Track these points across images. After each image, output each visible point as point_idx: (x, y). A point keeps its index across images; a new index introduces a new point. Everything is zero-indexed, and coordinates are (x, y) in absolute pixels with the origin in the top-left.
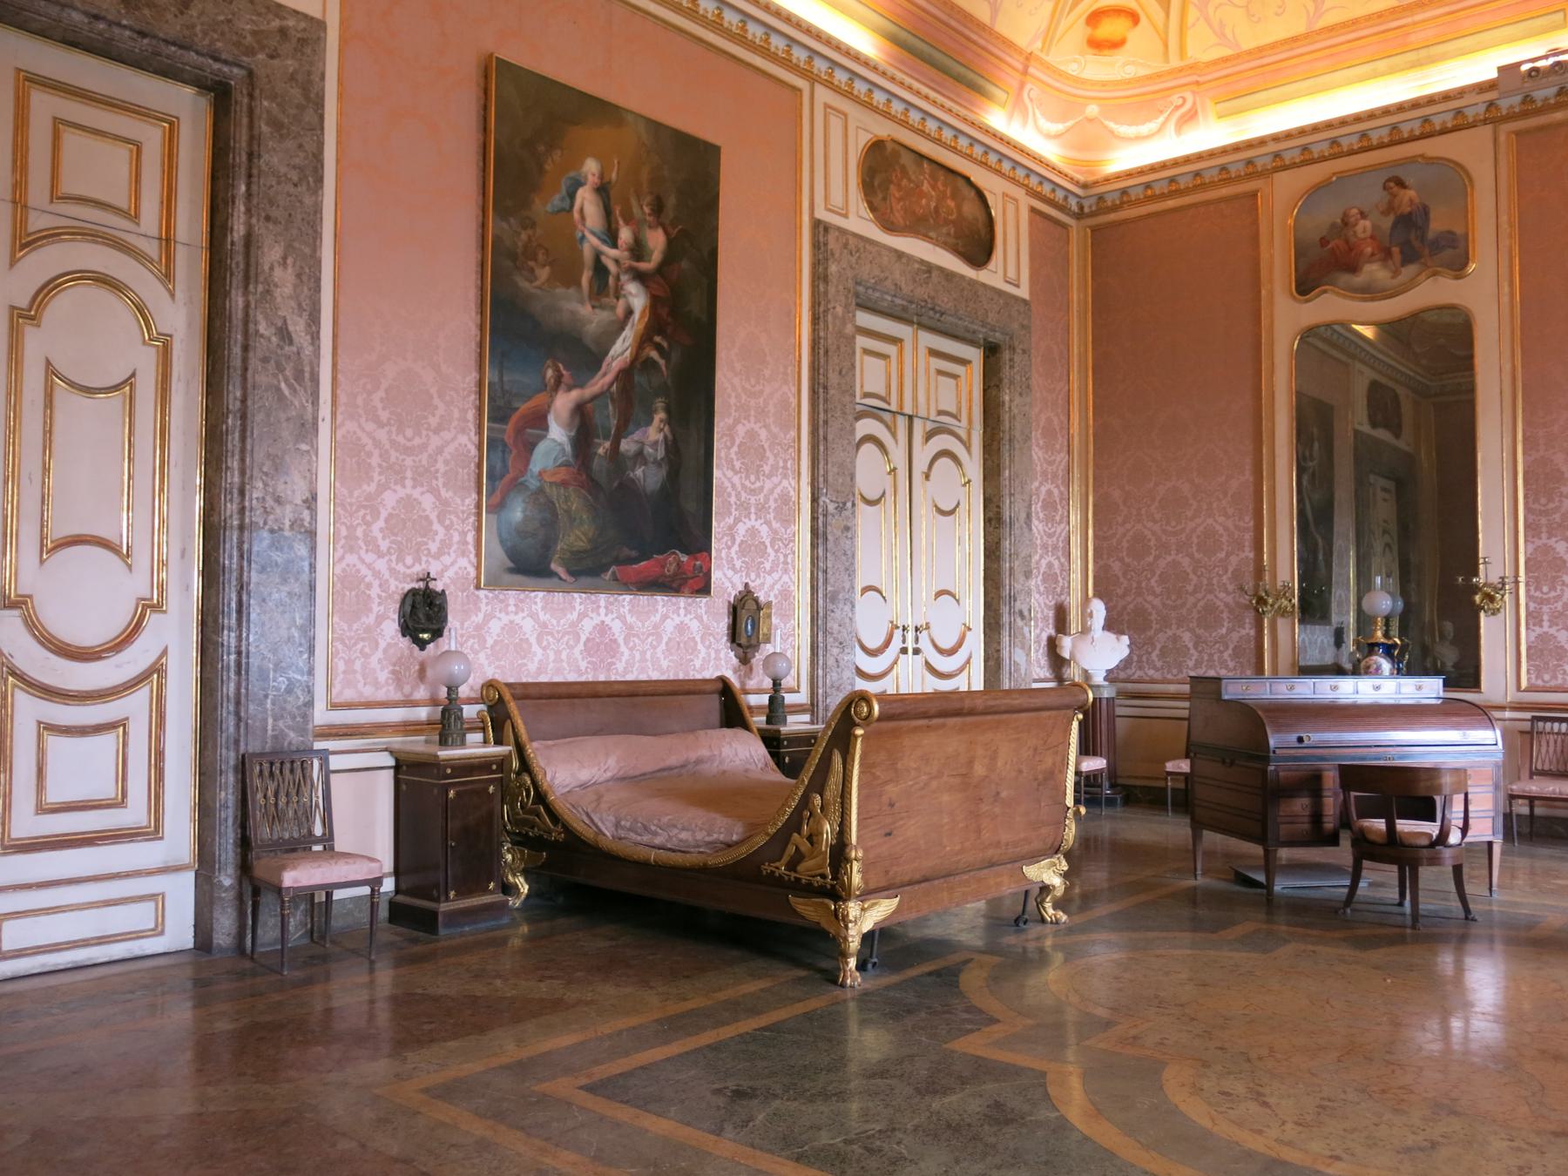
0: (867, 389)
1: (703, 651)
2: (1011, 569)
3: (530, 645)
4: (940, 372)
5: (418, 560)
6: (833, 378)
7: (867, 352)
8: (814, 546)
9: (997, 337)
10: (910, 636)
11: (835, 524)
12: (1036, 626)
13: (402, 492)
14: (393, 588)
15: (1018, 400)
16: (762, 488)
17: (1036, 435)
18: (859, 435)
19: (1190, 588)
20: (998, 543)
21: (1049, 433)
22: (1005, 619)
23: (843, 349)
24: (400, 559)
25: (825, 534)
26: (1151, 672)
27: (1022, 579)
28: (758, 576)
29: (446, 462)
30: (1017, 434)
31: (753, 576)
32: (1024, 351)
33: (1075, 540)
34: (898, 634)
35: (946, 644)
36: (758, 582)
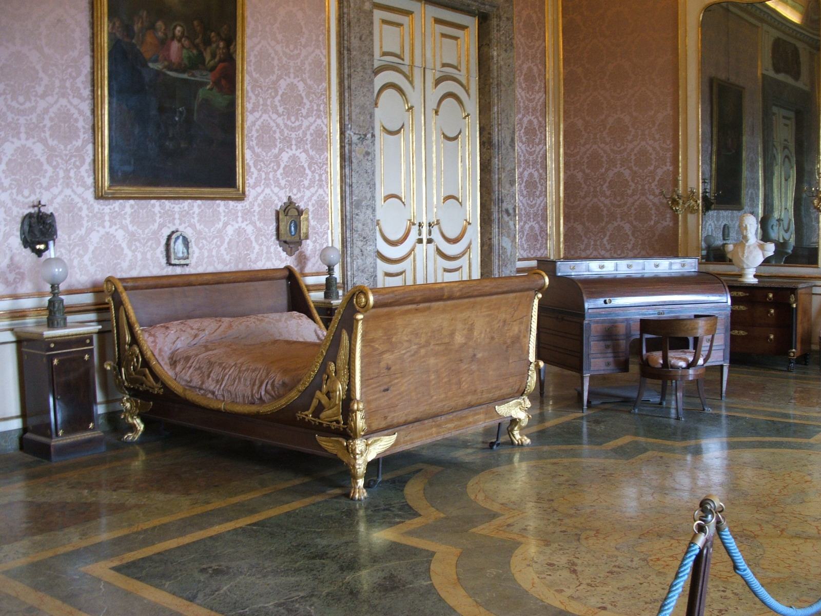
0: (385, 49)
1: (257, 247)
2: (499, 179)
3: (122, 249)
4: (444, 35)
5: (33, 192)
6: (355, 42)
7: (385, 22)
8: (342, 167)
9: (487, 8)
10: (425, 230)
11: (358, 152)
12: (520, 220)
13: (18, 143)
14: (15, 213)
15: (504, 55)
16: (301, 126)
17: (520, 80)
19: (629, 192)
20: (490, 160)
21: (530, 78)
22: (495, 216)
23: (362, 20)
24: (19, 192)
25: (350, 157)
26: (603, 253)
27: (508, 186)
28: (299, 190)
29: (51, 119)
30: (503, 80)
31: (295, 191)
32: (508, 19)
33: (551, 157)
34: (414, 230)
35: (452, 235)
36: (299, 195)
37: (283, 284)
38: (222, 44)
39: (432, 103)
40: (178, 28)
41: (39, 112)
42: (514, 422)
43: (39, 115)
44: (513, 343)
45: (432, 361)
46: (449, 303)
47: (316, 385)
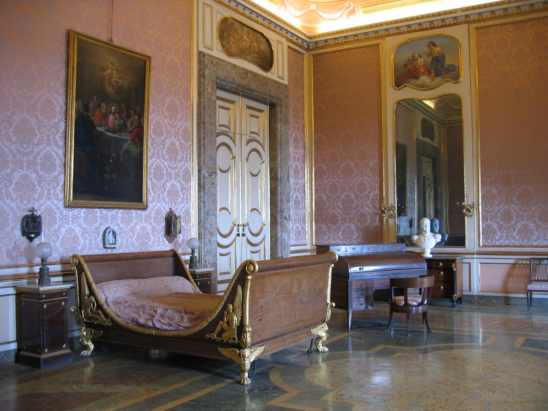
0: (221, 123)
1: (153, 238)
2: (281, 199)
3: (78, 238)
4: (251, 116)
5: (29, 202)
6: (207, 119)
8: (199, 191)
10: (241, 228)
11: (208, 182)
12: (292, 223)
13: (22, 173)
14: (18, 215)
15: (284, 127)
16: (177, 167)
17: (291, 141)
18: (218, 143)
19: (354, 206)
20: (276, 188)
21: (296, 141)
22: (279, 220)
23: (211, 106)
24: (22, 202)
25: (204, 186)
26: (339, 241)
27: (286, 203)
28: (176, 205)
29: (41, 159)
30: (283, 141)
31: (173, 205)
32: (286, 107)
33: (307, 186)
34: (236, 228)
35: (255, 231)
36: (176, 207)
37: (171, 260)
38: (136, 118)
39: (245, 155)
40: (113, 107)
41: (34, 154)
42: (319, 338)
43: (34, 156)
44: (320, 292)
45: (282, 303)
46: (291, 269)
47: (220, 317)
